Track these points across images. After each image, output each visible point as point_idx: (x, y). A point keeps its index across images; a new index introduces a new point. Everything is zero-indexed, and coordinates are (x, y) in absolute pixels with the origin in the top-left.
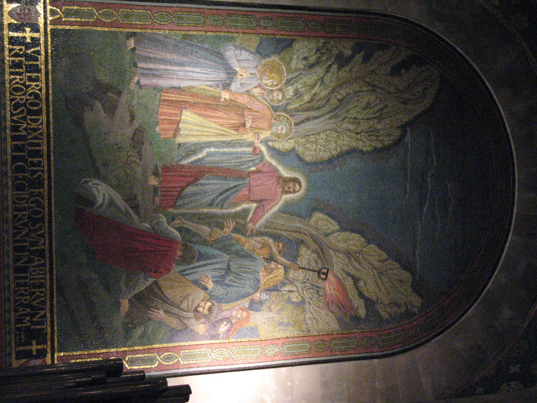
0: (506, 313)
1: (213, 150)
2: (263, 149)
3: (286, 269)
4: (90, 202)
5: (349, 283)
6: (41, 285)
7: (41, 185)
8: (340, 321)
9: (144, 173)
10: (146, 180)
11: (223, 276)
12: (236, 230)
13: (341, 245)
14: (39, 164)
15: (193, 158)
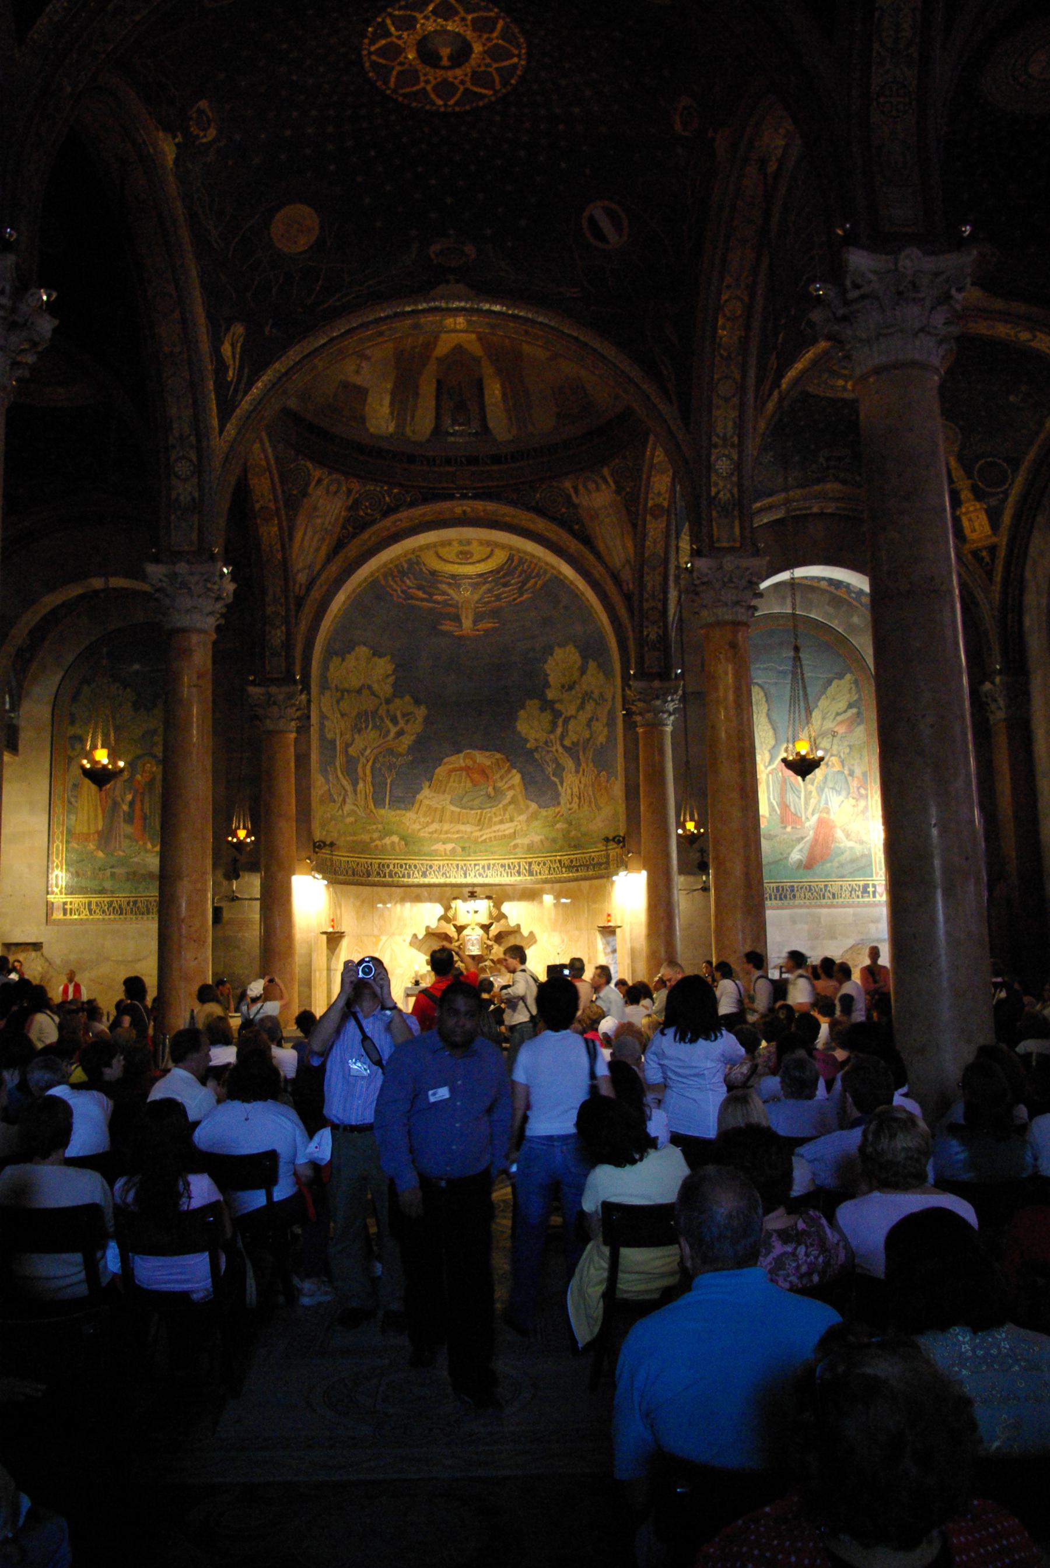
0: (855, 620)
1: (771, 797)
2: (770, 768)
3: (832, 755)
4: (801, 861)
5: (839, 718)
6: (841, 886)
7: (793, 886)
8: (859, 724)
9: (784, 834)
10: (789, 833)
11: (836, 791)
12: (812, 784)
13: (819, 723)
14: (782, 887)
15: (776, 807)
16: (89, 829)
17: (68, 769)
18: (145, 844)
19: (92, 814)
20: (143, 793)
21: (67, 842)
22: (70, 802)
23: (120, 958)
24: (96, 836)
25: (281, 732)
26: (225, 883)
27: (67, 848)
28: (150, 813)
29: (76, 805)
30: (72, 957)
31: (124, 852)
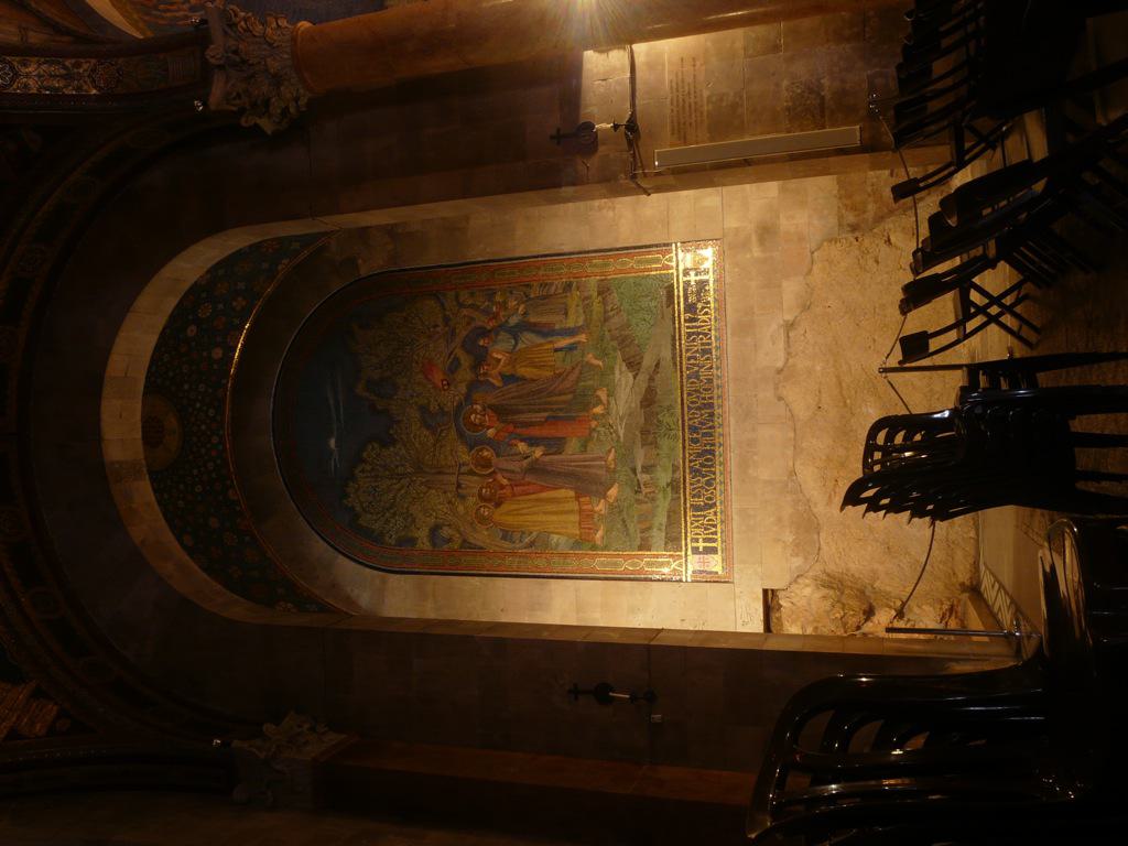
16: (571, 512)
17: (482, 548)
18: (595, 417)
19: (549, 508)
20: (516, 424)
21: (594, 547)
22: (532, 544)
23: (790, 452)
24: (582, 500)
25: (294, 39)
26: (602, 149)
27: (603, 550)
28: (545, 410)
29: (535, 534)
30: (789, 538)
31: (610, 451)
